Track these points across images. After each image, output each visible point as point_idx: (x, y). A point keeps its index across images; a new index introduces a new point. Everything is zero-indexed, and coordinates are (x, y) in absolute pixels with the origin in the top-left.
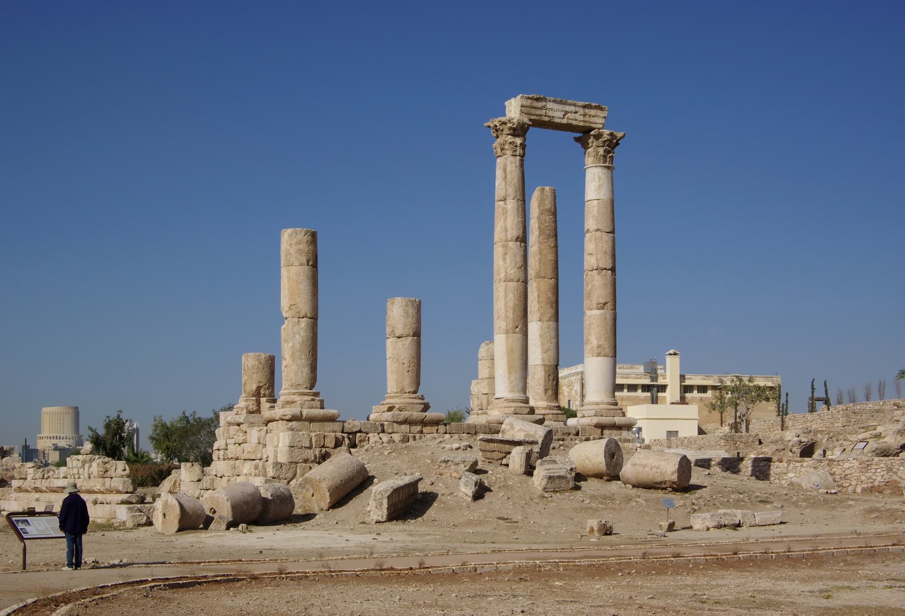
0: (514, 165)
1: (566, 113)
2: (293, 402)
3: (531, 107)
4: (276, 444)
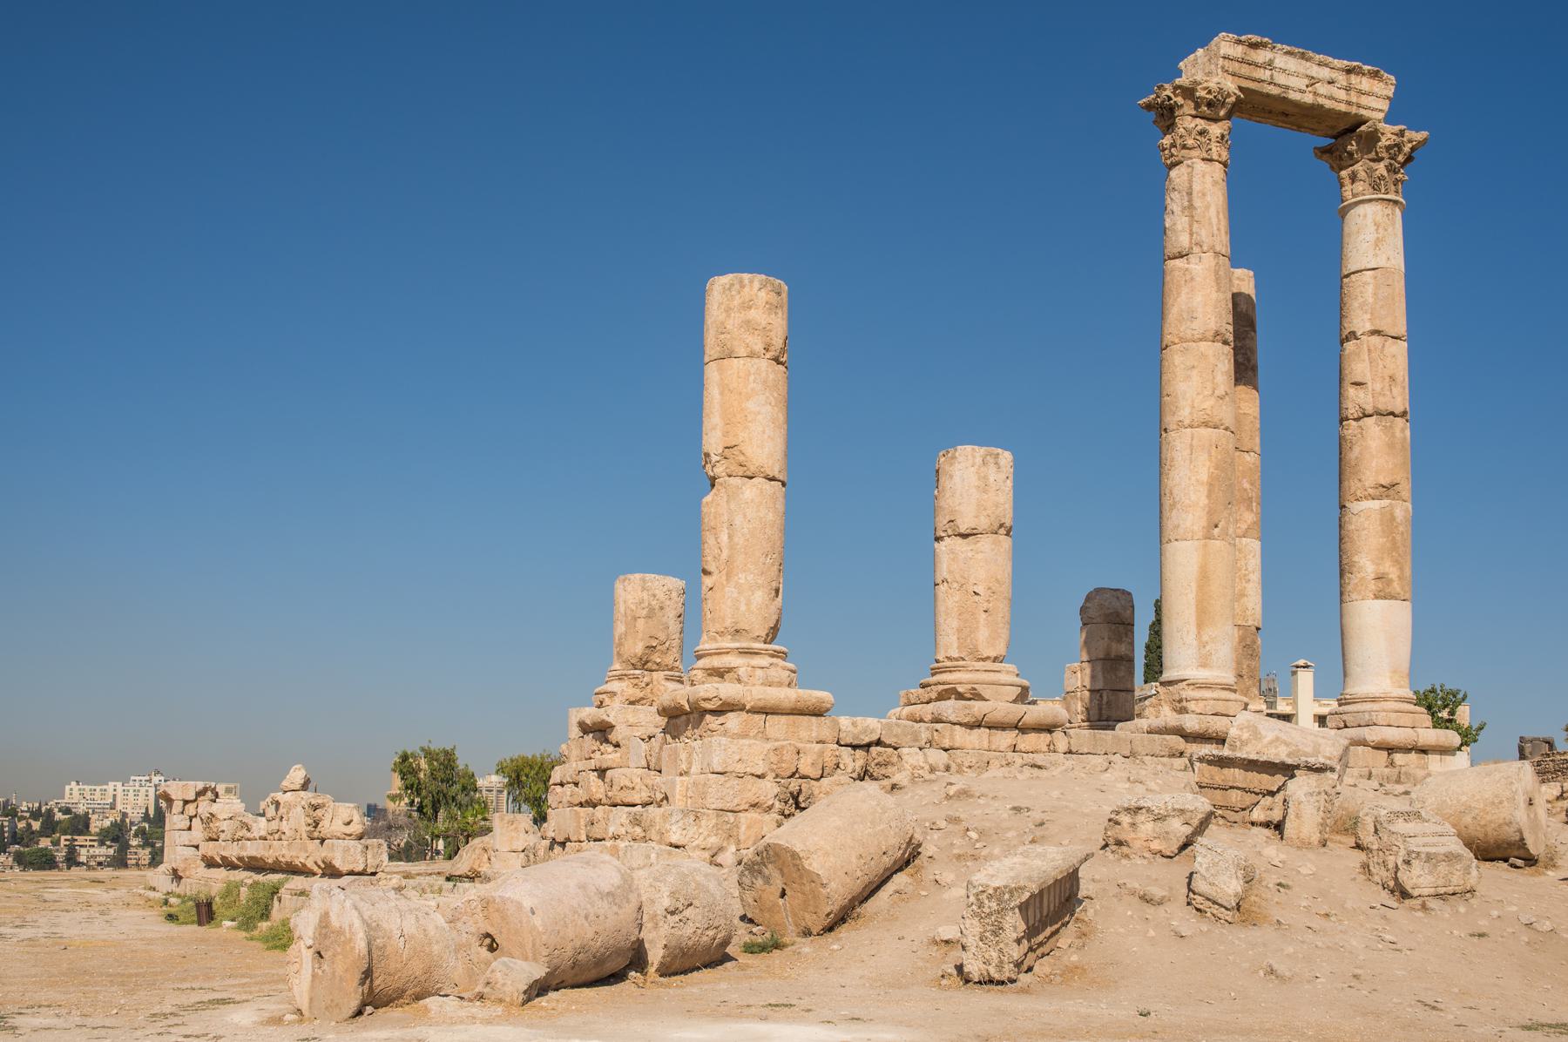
0: (1208, 180)
1: (1313, 82)
2: (730, 670)
3: (1242, 61)
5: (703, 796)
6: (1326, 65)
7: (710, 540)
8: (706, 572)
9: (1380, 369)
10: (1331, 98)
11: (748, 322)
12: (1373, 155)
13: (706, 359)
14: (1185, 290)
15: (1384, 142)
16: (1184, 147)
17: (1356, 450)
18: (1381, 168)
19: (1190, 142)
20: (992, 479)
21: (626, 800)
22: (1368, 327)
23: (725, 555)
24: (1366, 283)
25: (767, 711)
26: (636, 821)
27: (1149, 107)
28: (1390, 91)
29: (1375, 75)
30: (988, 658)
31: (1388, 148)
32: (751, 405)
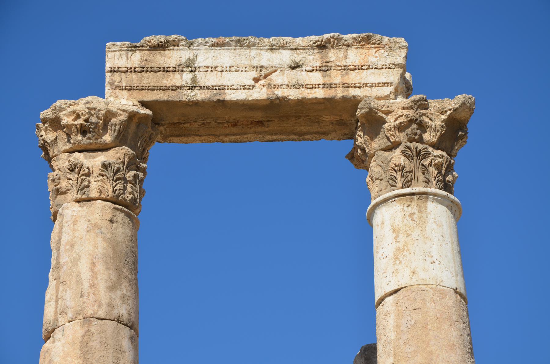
0: (83, 225)
6: (283, 47)
10: (297, 86)
15: (391, 121)
18: (397, 156)
28: (400, 57)
31: (401, 128)
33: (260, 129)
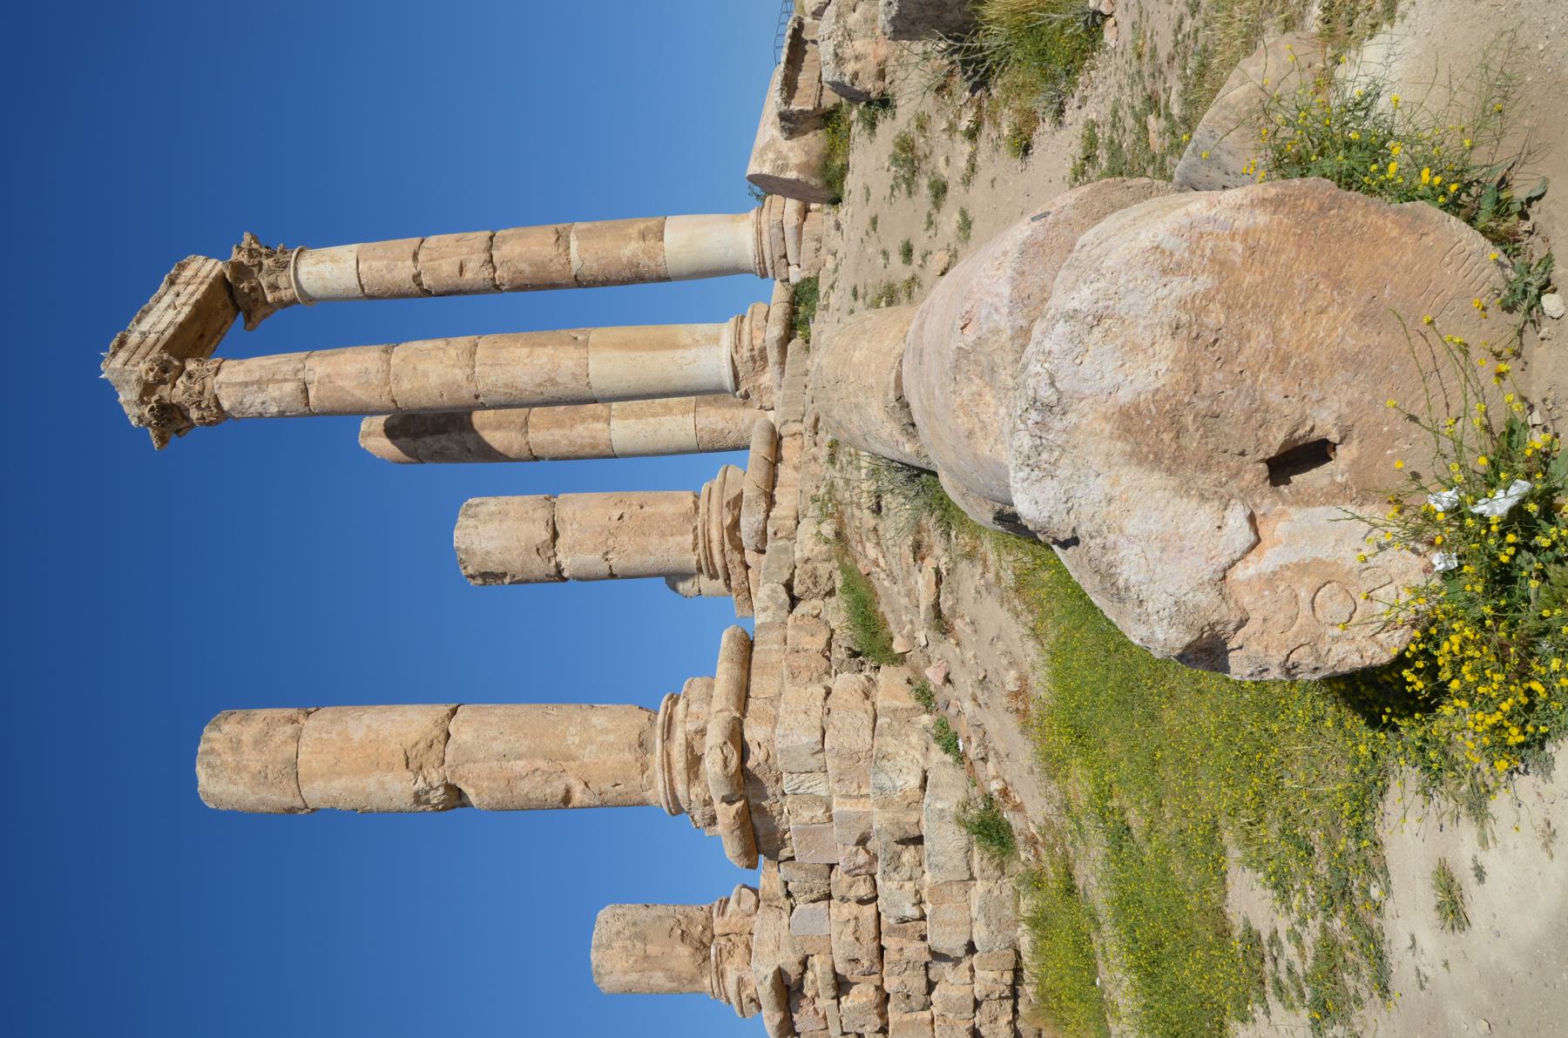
1: (172, 306)
2: (689, 746)
4: (820, 812)
5: (854, 756)
7: (525, 787)
8: (567, 798)
9: (450, 256)
11: (256, 742)
12: (255, 270)
13: (298, 803)
14: (340, 383)
15: (245, 260)
16: (201, 393)
17: (524, 266)
18: (267, 262)
19: (197, 388)
20: (493, 508)
21: (873, 930)
22: (410, 262)
23: (542, 764)
24: (370, 268)
25: (743, 695)
26: (895, 863)
27: (162, 439)
29: (182, 267)
30: (695, 503)
31: (251, 256)
32: (358, 735)
33: (206, 340)
